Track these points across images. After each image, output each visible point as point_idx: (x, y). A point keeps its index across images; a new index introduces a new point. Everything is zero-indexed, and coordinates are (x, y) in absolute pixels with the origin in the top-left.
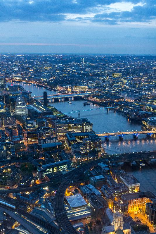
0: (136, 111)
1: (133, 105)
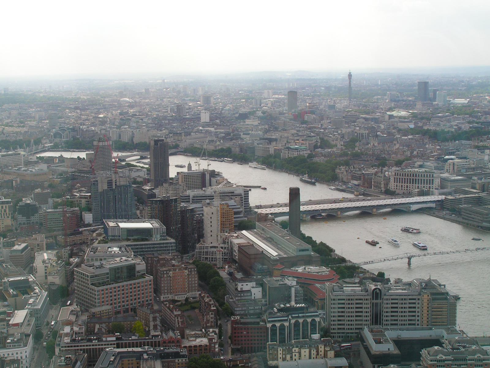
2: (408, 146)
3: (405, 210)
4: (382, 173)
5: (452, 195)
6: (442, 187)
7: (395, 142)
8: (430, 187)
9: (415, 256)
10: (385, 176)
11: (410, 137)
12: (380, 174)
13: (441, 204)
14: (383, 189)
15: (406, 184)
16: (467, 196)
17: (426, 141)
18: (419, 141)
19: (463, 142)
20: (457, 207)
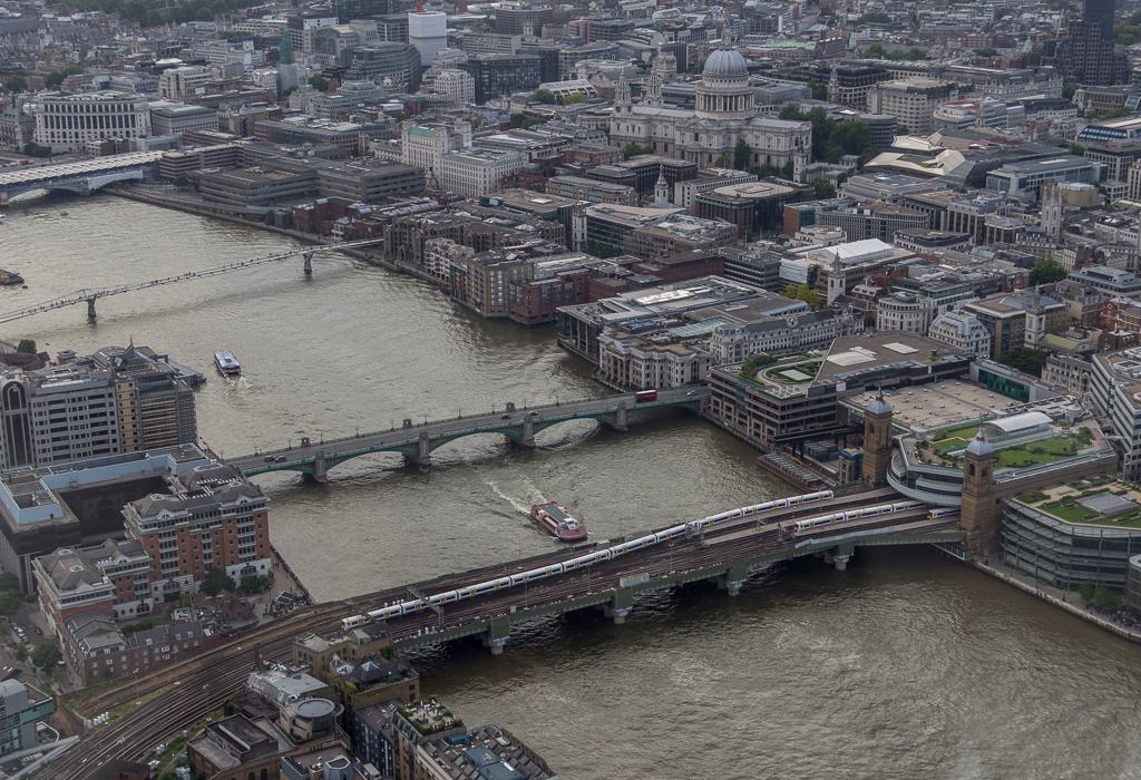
0: (511, 256)
1: (492, 220)
2: (73, 39)
3: (76, 189)
4: (14, 106)
5: (178, 149)
6: (156, 130)
7: (40, 31)
8: (128, 133)
9: (101, 294)
10: (23, 114)
11: (76, 17)
12: (9, 110)
13: (155, 172)
14: (21, 145)
15: (73, 130)
16: (209, 148)
17: (113, 25)
18: (97, 26)
19: (197, 24)
20: (190, 173)
